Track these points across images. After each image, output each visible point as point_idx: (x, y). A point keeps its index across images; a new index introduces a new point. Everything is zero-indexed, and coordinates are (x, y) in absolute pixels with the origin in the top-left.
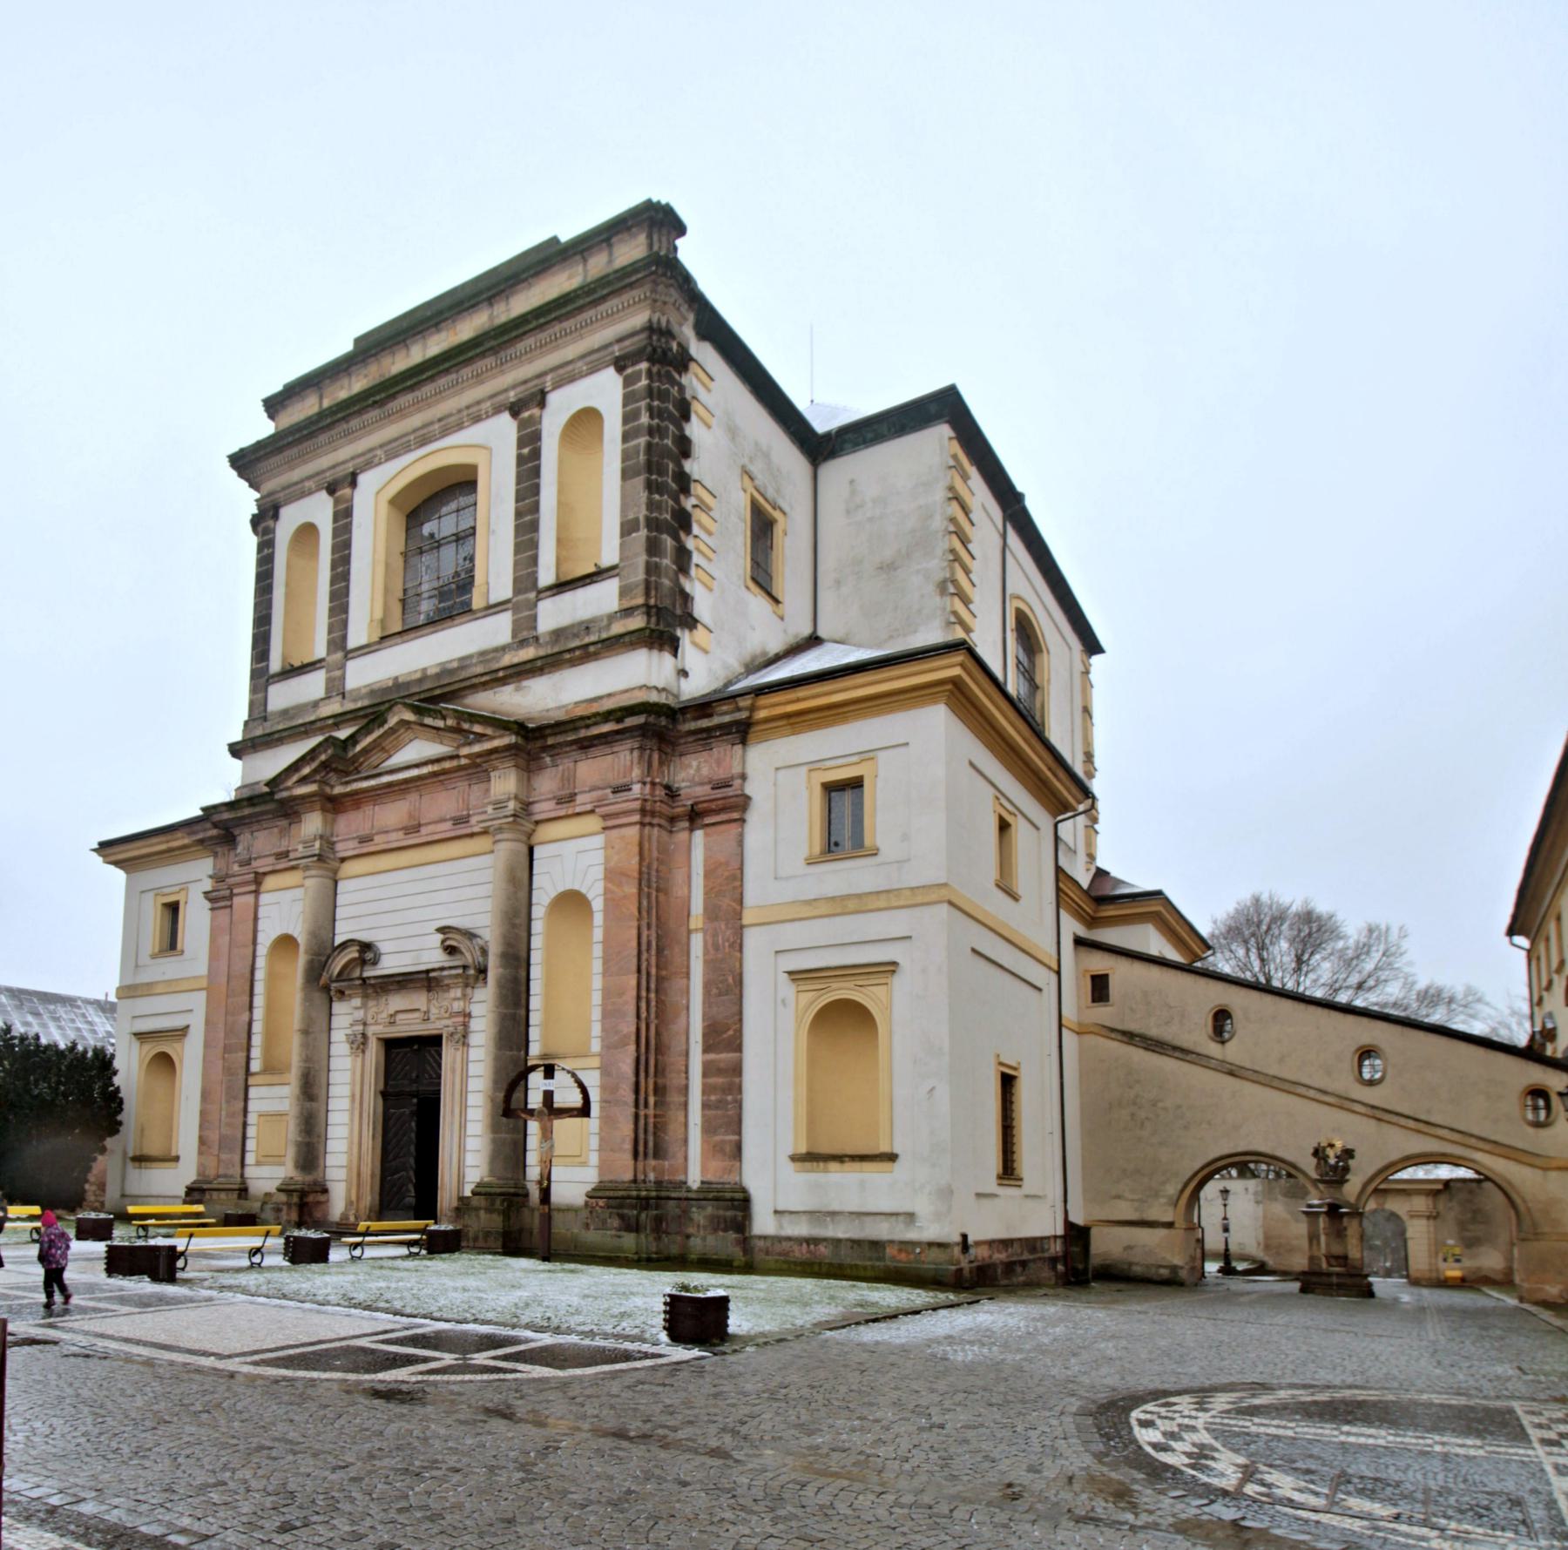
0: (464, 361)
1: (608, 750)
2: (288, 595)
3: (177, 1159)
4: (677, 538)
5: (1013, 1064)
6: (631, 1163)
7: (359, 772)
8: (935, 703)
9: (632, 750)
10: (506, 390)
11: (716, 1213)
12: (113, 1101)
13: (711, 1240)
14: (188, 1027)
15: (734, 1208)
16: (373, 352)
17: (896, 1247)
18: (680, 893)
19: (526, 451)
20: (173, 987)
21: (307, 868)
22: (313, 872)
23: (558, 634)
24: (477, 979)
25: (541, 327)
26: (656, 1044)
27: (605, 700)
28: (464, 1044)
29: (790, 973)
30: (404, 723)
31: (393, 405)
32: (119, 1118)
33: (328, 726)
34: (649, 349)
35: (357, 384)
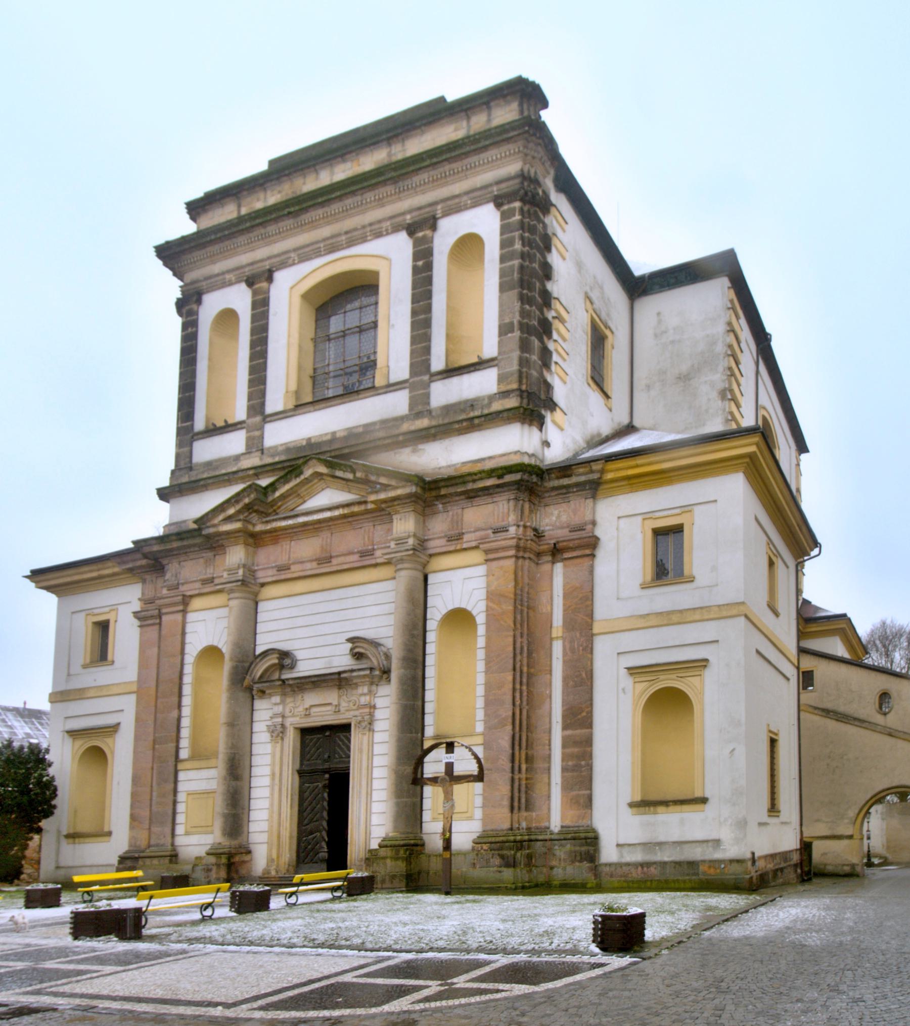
0: (369, 186)
1: (490, 500)
2: (211, 369)
3: (109, 834)
4: (541, 341)
5: (776, 731)
6: (510, 814)
7: (277, 514)
8: (737, 471)
10: (404, 214)
11: (573, 848)
12: (48, 789)
13: (570, 870)
14: (119, 724)
15: (587, 844)
16: (287, 172)
17: (707, 865)
18: (544, 611)
19: (420, 263)
20: (103, 692)
21: (231, 591)
23: (448, 409)
24: (381, 677)
25: (433, 165)
28: (370, 730)
29: (629, 669)
32: (53, 802)
33: (249, 476)
34: (522, 192)
35: (271, 198)
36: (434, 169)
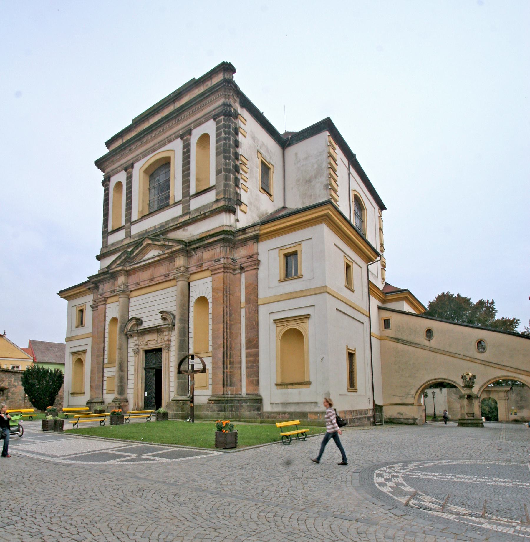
1: (213, 248)
4: (235, 175)
8: (321, 223)
9: (220, 247)
10: (179, 131)
19: (185, 150)
21: (120, 295)
22: (122, 296)
24: (172, 328)
26: (230, 348)
27: (211, 231)
29: (274, 320)
30: (149, 245)
31: (144, 140)
34: (224, 111)
35: (133, 134)
36: (190, 109)
